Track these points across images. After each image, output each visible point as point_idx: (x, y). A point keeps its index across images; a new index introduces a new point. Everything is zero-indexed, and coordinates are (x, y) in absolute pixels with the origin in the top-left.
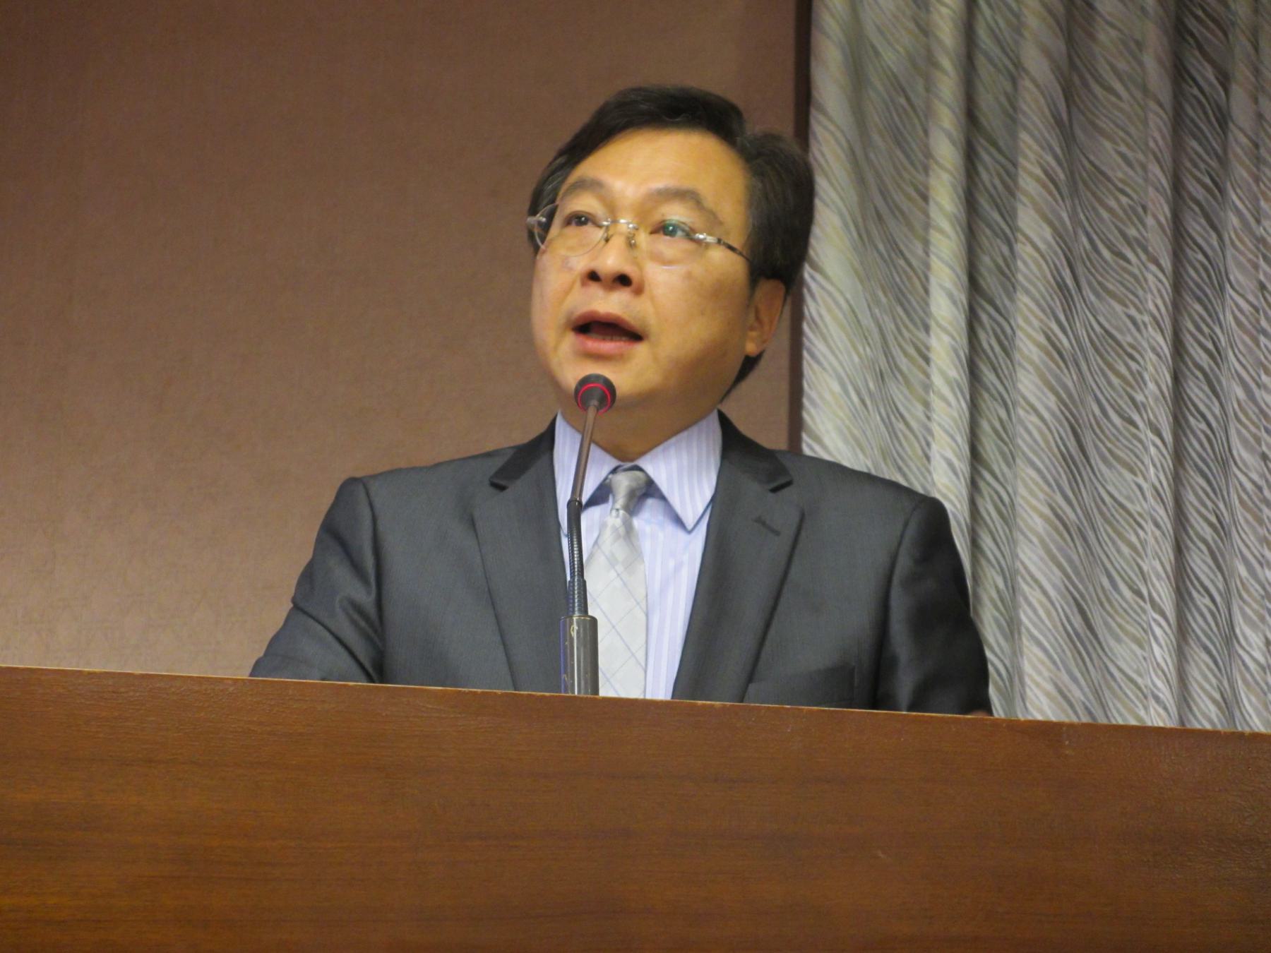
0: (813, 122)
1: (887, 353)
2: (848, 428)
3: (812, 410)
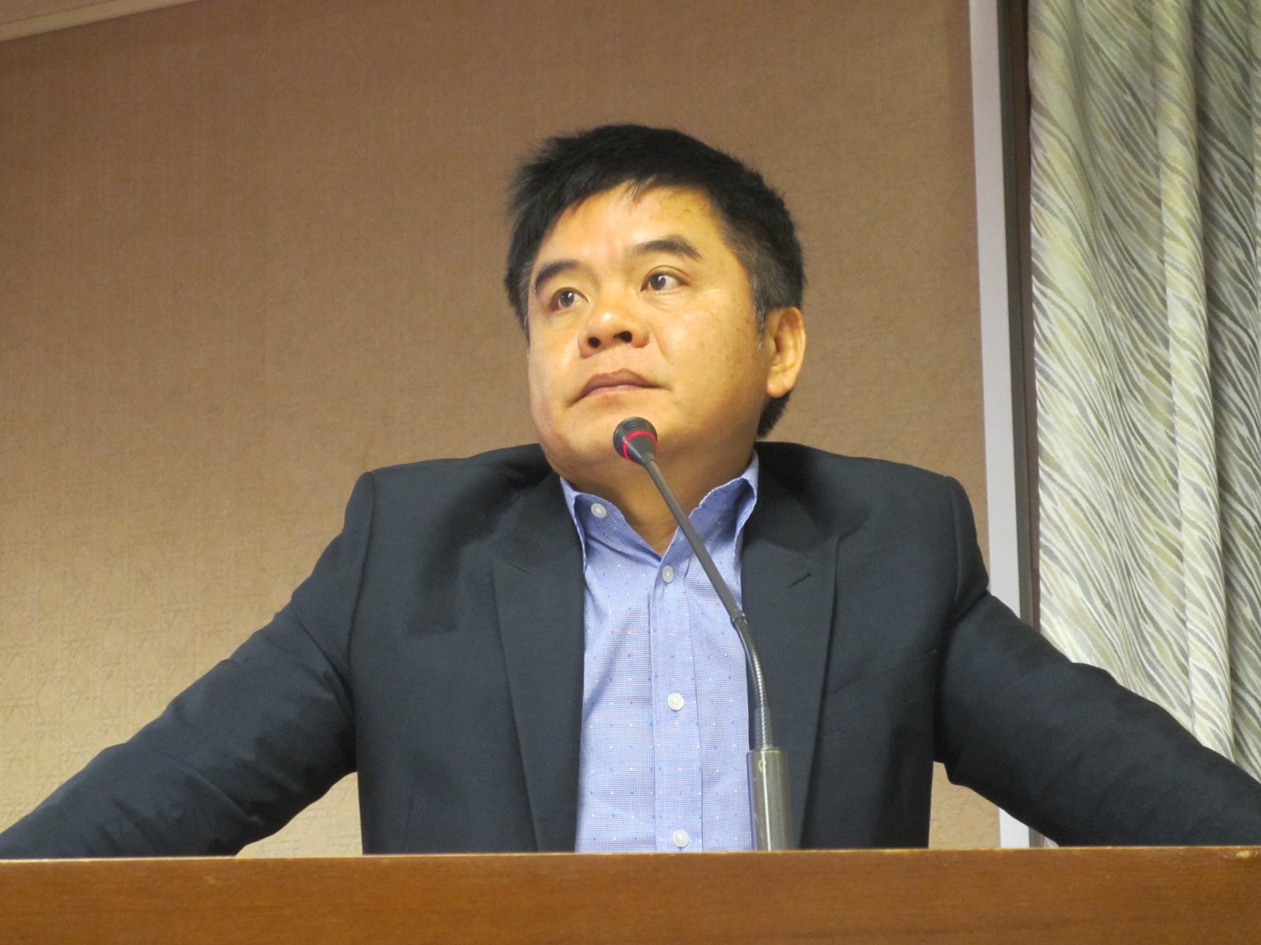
0: (1034, 124)
1: (1123, 369)
2: (1087, 453)
3: (1050, 437)
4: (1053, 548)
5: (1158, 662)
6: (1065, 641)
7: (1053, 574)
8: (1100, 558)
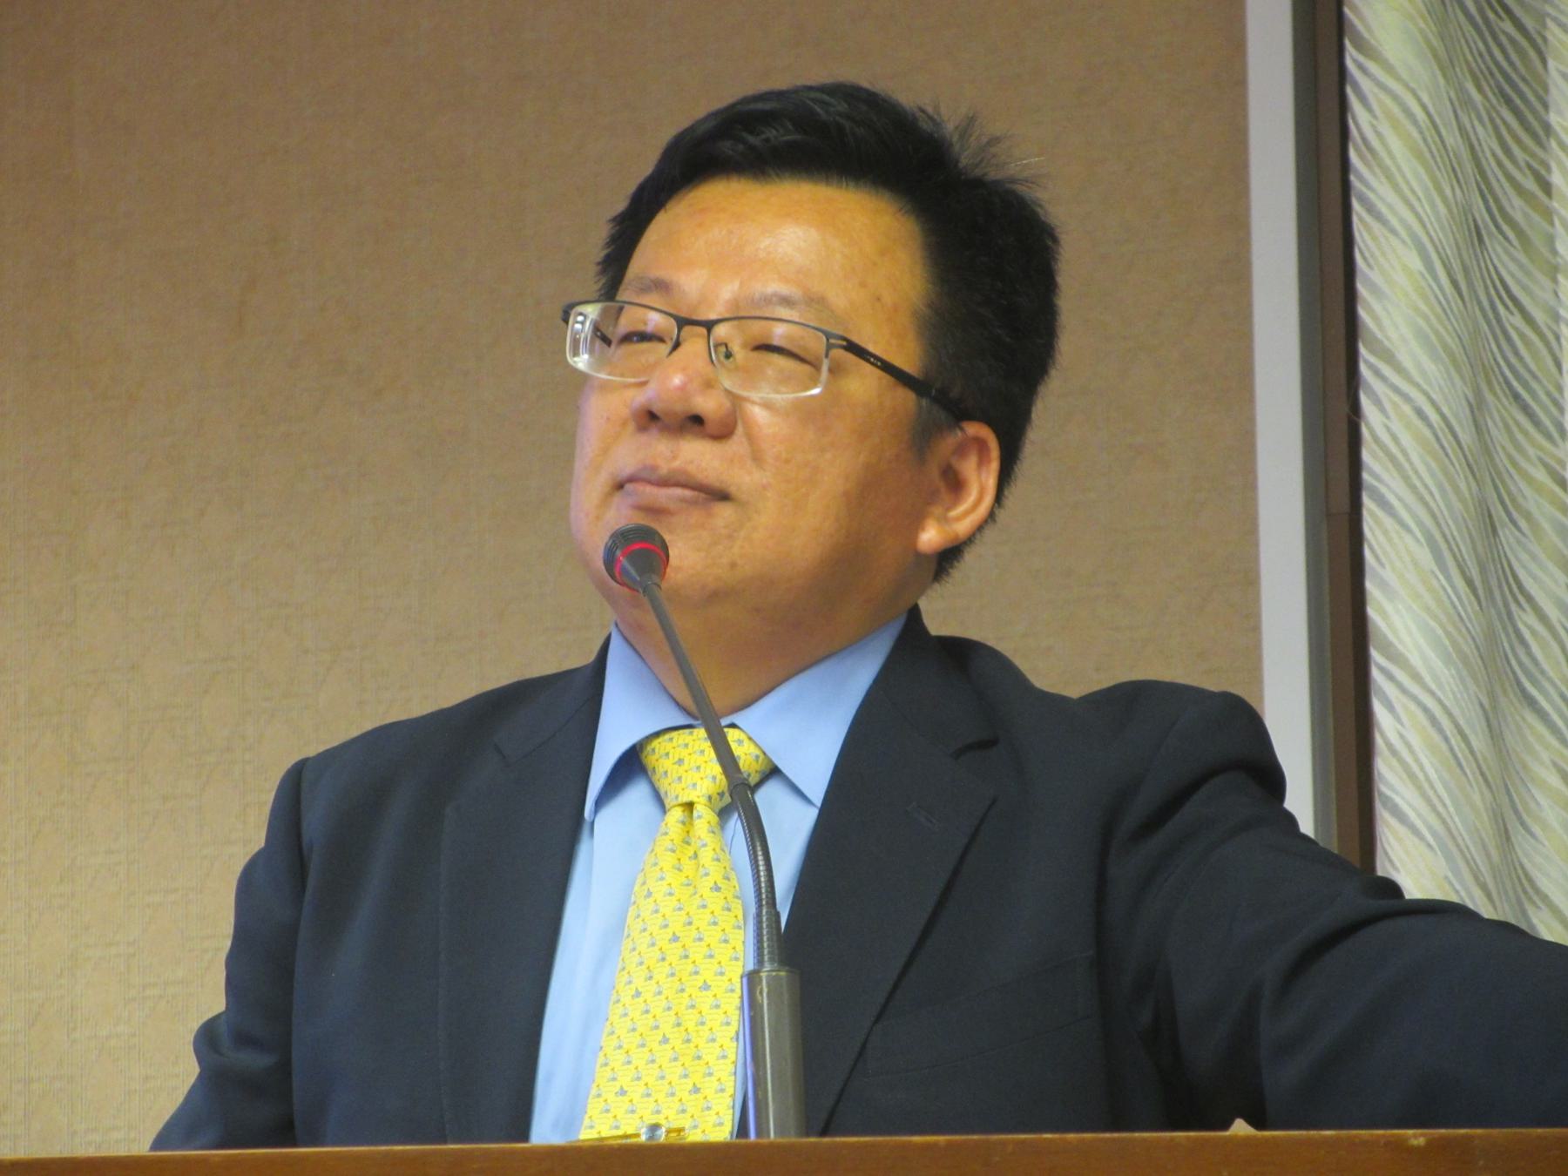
2: (1437, 333)
3: (1377, 307)
4: (1383, 490)
5: (1543, 672)
6: (1407, 639)
7: (1385, 532)
8: (1458, 506)
